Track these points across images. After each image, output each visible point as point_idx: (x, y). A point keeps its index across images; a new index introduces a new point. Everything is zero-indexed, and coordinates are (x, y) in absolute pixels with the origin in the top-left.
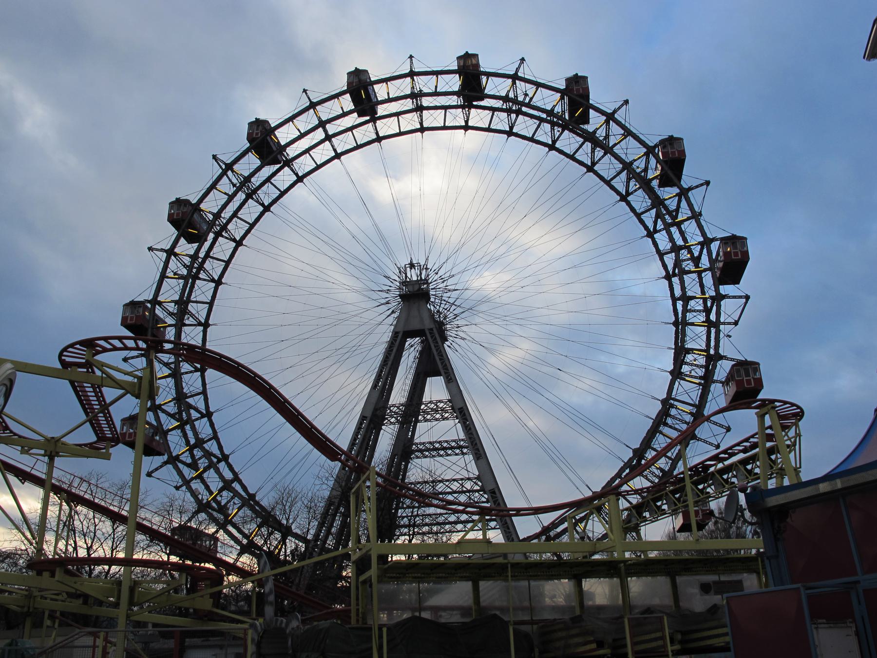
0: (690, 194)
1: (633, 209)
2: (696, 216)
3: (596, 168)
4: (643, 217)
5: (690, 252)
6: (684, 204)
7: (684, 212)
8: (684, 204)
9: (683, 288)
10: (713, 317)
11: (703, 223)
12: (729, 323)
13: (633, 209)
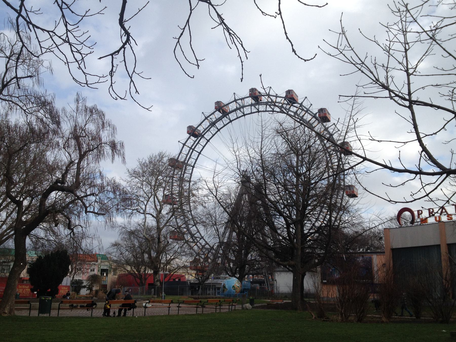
0: (270, 94)
1: (263, 111)
2: (277, 96)
3: (245, 113)
4: (267, 110)
5: (285, 104)
6: (271, 97)
7: (274, 99)
8: (271, 97)
9: (292, 112)
10: (305, 109)
11: (280, 96)
12: (310, 106)
13: (263, 111)
